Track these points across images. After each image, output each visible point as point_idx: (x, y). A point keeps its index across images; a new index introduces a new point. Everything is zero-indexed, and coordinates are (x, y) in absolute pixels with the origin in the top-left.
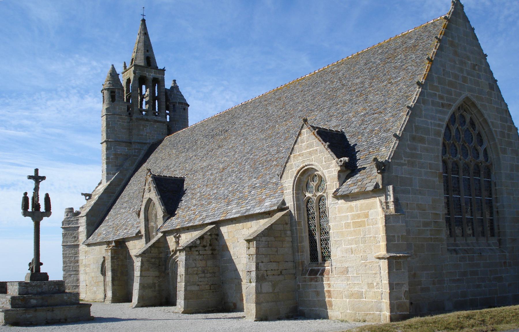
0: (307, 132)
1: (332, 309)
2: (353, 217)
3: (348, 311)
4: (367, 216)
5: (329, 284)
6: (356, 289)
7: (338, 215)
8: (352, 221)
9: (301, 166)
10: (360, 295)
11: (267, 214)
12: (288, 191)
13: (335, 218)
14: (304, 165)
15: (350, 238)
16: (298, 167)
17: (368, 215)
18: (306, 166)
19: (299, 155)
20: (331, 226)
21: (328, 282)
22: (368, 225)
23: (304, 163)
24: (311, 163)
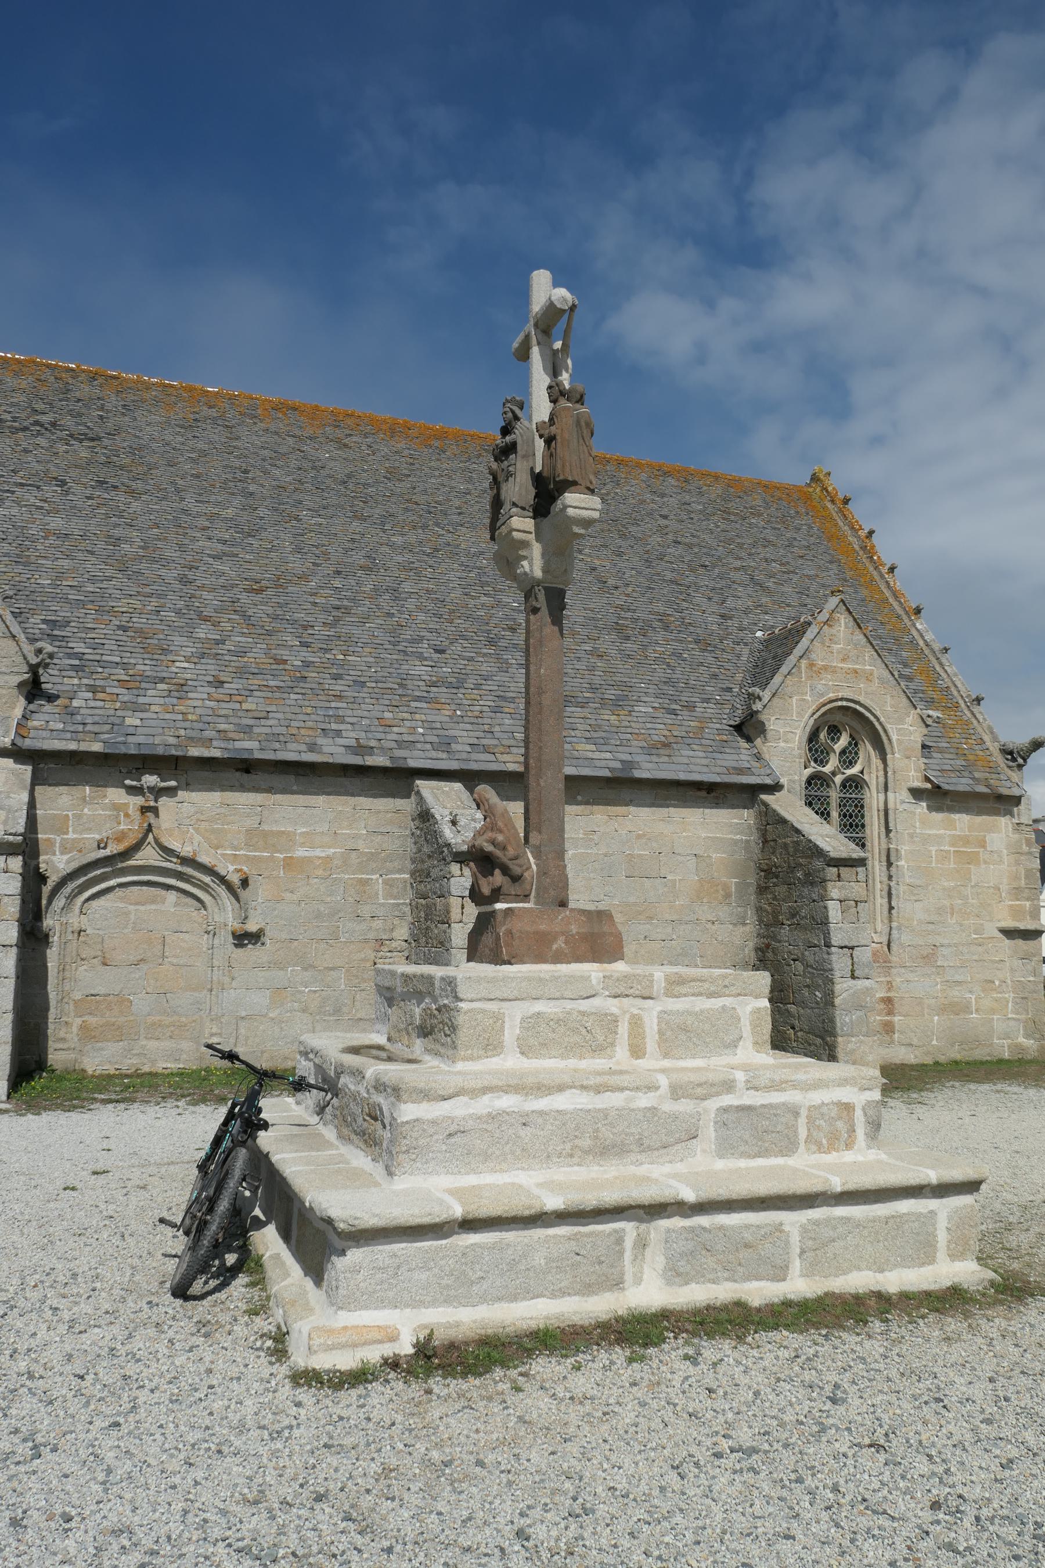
0: (846, 623)
1: (892, 1042)
2: (955, 840)
3: (934, 1042)
4: (983, 844)
5: (888, 982)
6: (957, 993)
7: (918, 831)
8: (952, 849)
9: (832, 695)
10: (959, 1008)
11: (699, 789)
12: (782, 744)
13: (911, 836)
14: (840, 695)
15: (946, 884)
16: (822, 695)
17: (985, 842)
18: (841, 699)
19: (825, 668)
20: (903, 853)
21: (889, 979)
22: (985, 862)
23: (838, 691)
24: (856, 698)
